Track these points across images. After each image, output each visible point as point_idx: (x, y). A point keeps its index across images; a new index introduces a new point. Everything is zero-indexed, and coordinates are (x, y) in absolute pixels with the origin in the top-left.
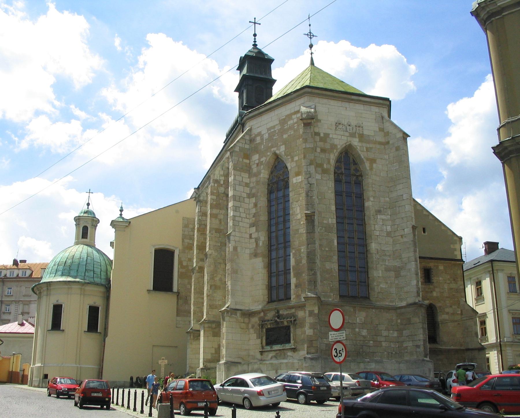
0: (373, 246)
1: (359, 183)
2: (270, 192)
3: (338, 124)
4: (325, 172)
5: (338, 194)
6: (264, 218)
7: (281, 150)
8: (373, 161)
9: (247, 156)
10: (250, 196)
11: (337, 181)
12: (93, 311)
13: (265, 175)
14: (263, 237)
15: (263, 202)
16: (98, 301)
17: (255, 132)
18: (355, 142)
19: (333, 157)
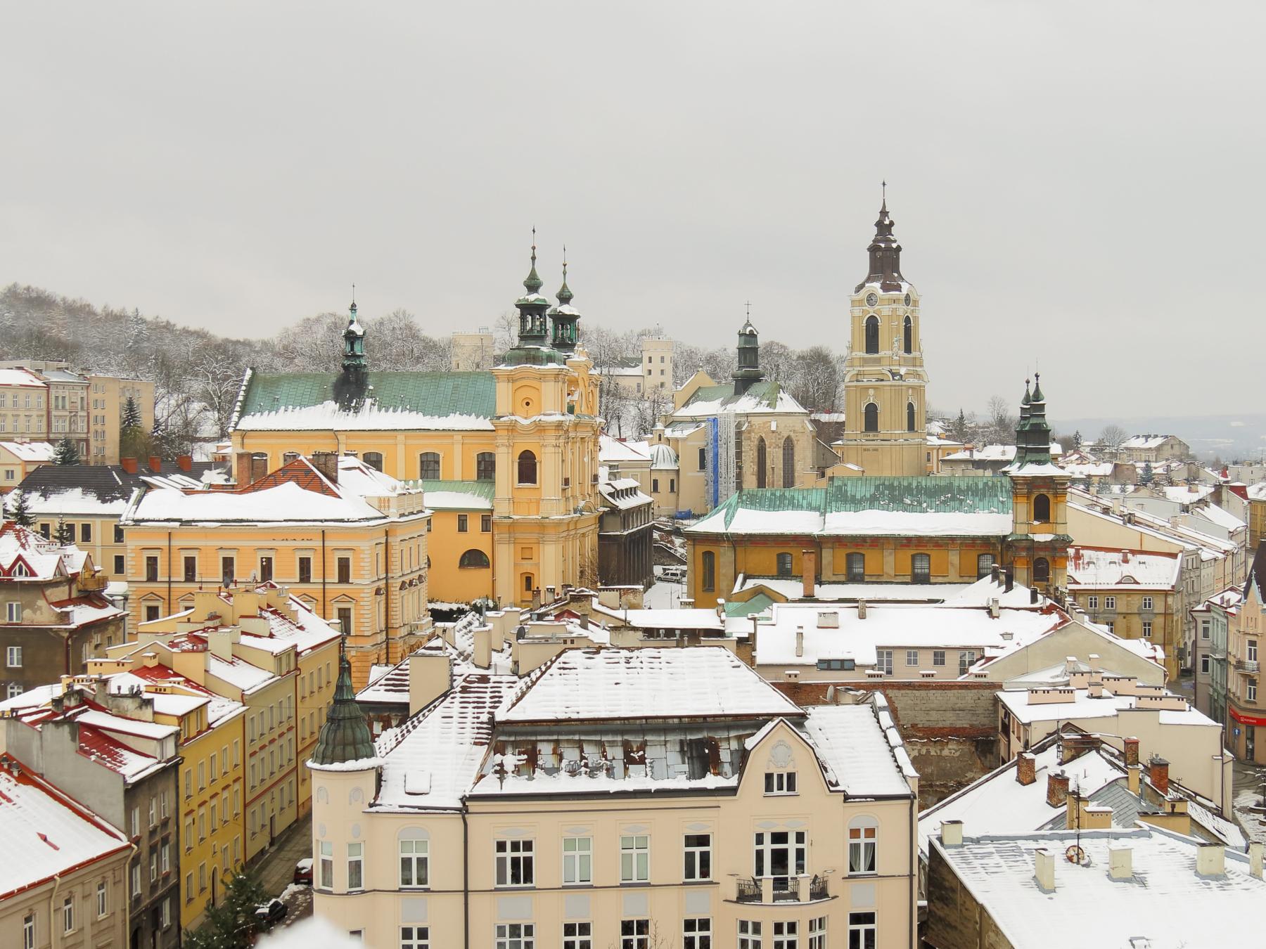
0: (796, 474)
1: (792, 449)
2: (759, 450)
3: (786, 426)
4: (780, 447)
5: (784, 454)
6: (756, 460)
7: (763, 436)
8: (798, 441)
9: (749, 433)
10: (751, 450)
11: (784, 449)
12: (672, 481)
13: (756, 442)
14: (756, 468)
15: (756, 454)
16: (674, 476)
17: (752, 423)
18: (792, 434)
19: (782, 441)
